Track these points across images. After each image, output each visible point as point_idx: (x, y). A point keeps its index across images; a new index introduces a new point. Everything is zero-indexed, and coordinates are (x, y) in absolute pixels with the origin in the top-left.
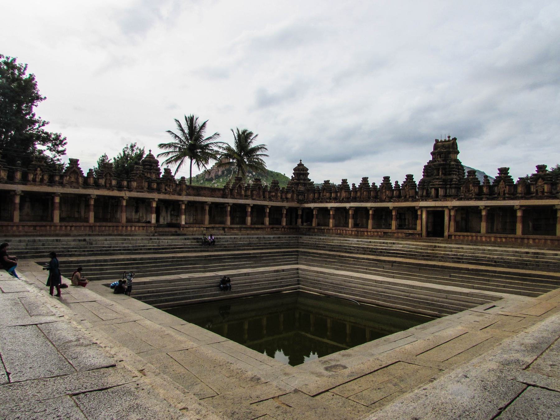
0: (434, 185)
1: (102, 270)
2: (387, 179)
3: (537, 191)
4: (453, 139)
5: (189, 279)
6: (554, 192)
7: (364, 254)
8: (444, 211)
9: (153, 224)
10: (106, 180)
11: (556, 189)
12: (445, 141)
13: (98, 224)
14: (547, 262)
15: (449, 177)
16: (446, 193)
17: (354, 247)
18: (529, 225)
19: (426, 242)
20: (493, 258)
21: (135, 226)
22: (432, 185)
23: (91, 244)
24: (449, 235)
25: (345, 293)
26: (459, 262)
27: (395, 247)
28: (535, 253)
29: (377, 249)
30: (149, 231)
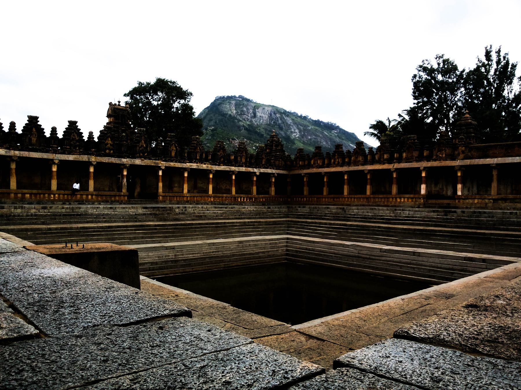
1: (316, 230)
5: (348, 246)
9: (423, 195)
10: (380, 155)
13: (372, 196)
21: (404, 198)
23: (345, 212)
30: (417, 203)
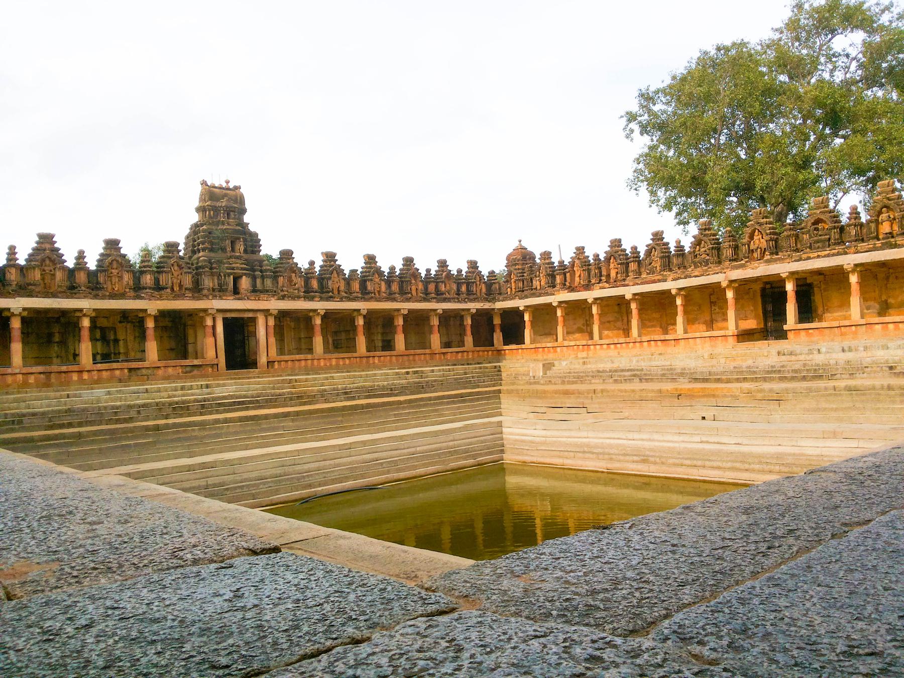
0: (233, 269)
2: (112, 245)
7: (167, 417)
8: (254, 320)
12: (221, 188)
15: (254, 257)
17: (117, 408)
19: (235, 379)
20: (383, 386)
22: (227, 268)
25: (320, 486)
26: (353, 398)
27: (219, 392)
29: (183, 402)
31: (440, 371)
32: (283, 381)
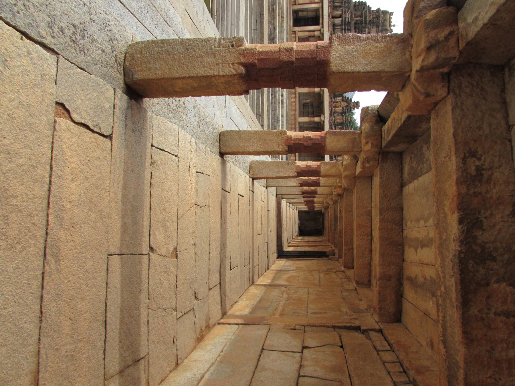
0: (345, 13)
3: (337, 102)
4: (391, 29)
6: (335, 115)
8: (318, 24)
11: (338, 116)
12: (390, 22)
14: (275, 109)
15: (353, 28)
16: (337, 25)
18: (308, 99)
19: (287, 9)
22: (345, 11)
24: (295, 32)
26: (269, 39)
28: (282, 101)
31: (282, 122)
32: (283, 13)
